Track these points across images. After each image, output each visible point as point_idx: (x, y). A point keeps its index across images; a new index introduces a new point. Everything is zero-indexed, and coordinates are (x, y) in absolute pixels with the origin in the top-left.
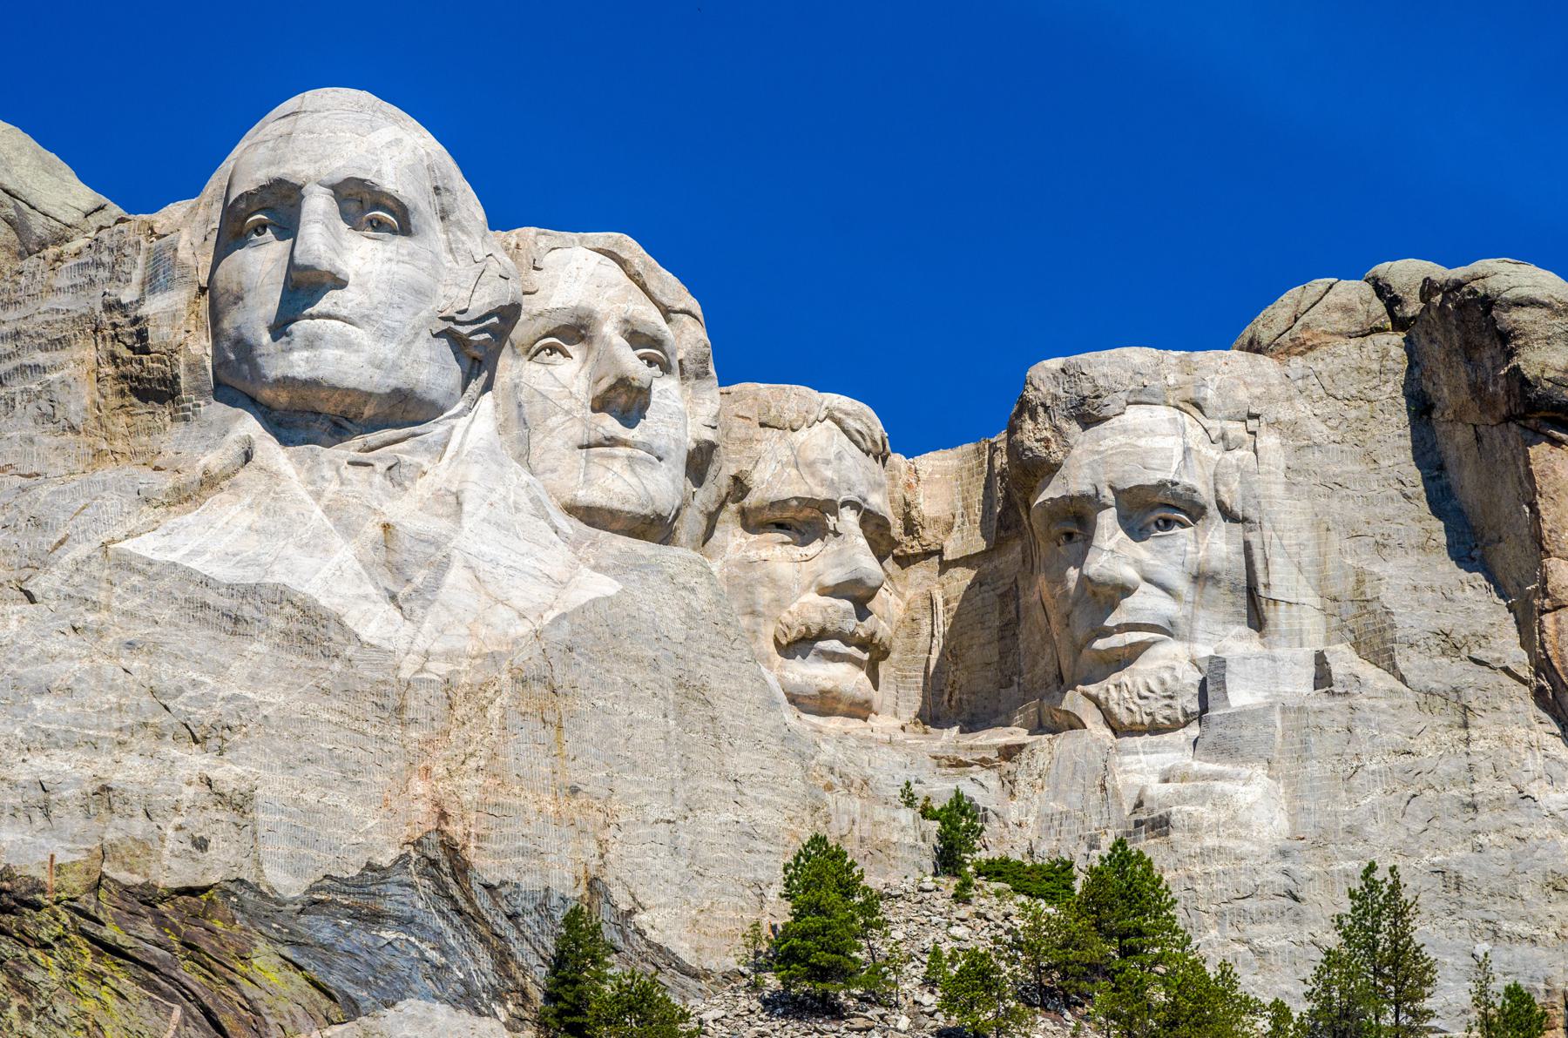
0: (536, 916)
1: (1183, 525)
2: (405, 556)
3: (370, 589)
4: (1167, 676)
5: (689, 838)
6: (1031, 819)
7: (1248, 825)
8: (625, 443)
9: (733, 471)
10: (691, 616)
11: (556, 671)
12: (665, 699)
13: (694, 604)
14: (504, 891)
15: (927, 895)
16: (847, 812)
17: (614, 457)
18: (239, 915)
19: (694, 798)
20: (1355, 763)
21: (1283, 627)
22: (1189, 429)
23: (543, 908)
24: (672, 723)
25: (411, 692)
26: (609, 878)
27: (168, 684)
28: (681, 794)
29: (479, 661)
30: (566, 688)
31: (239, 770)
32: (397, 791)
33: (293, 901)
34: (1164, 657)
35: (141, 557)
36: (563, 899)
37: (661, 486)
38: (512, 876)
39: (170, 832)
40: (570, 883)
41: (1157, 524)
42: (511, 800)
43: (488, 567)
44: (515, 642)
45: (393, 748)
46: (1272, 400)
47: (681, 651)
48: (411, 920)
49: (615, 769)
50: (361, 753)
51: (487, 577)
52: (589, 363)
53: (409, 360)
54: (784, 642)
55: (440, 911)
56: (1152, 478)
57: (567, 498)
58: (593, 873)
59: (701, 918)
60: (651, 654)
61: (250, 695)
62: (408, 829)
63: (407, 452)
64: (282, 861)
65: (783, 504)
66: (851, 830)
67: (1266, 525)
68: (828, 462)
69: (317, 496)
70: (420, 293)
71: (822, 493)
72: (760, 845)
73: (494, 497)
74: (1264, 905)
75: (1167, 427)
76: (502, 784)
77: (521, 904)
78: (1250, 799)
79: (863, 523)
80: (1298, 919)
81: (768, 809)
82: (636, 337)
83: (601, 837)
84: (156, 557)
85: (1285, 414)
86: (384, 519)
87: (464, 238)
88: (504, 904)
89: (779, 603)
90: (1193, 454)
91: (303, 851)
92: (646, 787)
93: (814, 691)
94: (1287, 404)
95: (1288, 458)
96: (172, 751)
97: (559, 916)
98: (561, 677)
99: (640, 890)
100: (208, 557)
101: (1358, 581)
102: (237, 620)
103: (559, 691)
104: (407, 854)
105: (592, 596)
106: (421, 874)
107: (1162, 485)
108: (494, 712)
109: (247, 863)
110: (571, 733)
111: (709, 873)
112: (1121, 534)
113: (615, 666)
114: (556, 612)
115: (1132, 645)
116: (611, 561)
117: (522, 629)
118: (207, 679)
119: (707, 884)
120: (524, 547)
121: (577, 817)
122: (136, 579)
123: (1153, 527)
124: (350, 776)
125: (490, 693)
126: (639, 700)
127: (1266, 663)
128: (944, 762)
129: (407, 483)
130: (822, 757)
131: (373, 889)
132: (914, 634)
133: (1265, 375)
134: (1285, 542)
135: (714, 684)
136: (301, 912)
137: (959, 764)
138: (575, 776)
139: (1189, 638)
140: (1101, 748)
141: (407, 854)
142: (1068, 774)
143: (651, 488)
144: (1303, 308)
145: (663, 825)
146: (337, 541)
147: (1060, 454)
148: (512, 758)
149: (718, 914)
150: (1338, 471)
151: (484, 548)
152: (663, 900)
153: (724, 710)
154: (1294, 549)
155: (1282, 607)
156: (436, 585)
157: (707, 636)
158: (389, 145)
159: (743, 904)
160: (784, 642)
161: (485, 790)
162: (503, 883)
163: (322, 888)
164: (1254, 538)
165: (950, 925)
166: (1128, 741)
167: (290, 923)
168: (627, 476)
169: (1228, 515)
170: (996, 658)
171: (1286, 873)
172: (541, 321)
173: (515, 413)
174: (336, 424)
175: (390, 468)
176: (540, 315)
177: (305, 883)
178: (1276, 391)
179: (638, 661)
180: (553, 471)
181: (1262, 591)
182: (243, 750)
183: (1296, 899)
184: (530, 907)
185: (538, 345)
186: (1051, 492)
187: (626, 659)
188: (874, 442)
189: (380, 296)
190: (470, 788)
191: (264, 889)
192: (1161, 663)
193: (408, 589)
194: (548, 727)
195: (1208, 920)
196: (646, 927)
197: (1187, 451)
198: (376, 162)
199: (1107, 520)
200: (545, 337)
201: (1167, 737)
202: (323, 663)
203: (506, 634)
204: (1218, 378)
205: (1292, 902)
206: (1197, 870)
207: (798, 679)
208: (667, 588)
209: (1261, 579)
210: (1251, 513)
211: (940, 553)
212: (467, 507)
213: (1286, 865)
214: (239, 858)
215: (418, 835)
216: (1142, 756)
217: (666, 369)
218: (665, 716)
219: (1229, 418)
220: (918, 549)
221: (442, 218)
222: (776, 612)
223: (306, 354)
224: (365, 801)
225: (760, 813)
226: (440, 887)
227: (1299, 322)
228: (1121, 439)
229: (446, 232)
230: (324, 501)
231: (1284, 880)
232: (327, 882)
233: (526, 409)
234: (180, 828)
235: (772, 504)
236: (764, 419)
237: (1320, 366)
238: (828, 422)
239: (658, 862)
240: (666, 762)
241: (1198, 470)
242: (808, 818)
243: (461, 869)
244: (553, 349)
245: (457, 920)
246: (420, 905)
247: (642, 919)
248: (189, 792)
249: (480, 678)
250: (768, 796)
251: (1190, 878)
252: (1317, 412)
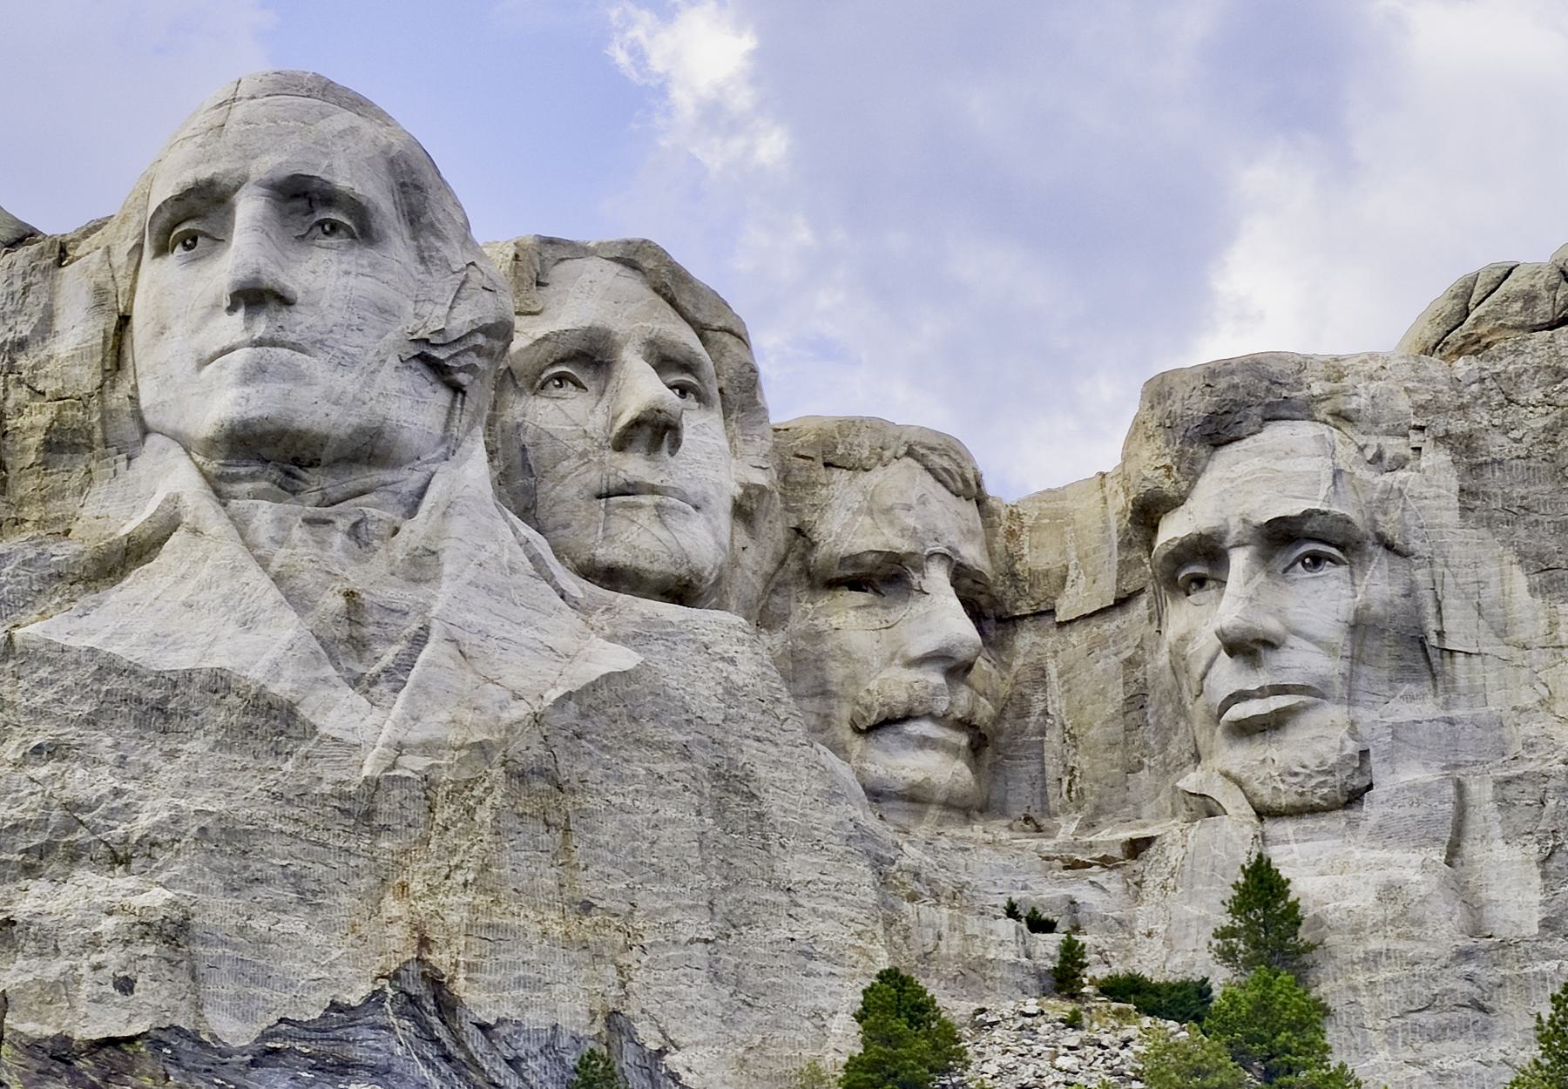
0: (542, 1060)
1: (1335, 561)
2: (372, 629)
3: (329, 671)
4: (1322, 747)
5: (733, 960)
6: (1160, 928)
7: (1420, 923)
8: (653, 490)
9: (794, 522)
10: (731, 691)
11: (561, 762)
12: (701, 794)
13: (733, 677)
14: (504, 1031)
15: (1029, 1020)
16: (931, 925)
17: (640, 506)
18: (172, 1070)
19: (739, 912)
20: (1551, 843)
21: (1462, 683)
22: (1339, 447)
23: (549, 1048)
24: (709, 821)
25: (381, 794)
26: (632, 1010)
27: (85, 793)
28: (721, 907)
29: (464, 753)
30: (575, 783)
31: (169, 895)
32: (367, 914)
33: (241, 1051)
34: (1318, 725)
35: (49, 642)
36: (576, 1039)
37: (702, 540)
38: (508, 1010)
39: (84, 970)
40: (584, 1019)
41: (1304, 564)
42: (507, 920)
43: (476, 640)
44: (510, 728)
45: (360, 862)
46: (1440, 409)
47: (718, 734)
48: (388, 1070)
49: (637, 879)
50: (320, 869)
51: (474, 652)
52: (607, 395)
53: (374, 393)
54: (863, 727)
55: (423, 1058)
56: (1294, 508)
57: (584, 557)
58: (612, 1006)
59: (750, 1056)
60: (680, 738)
61: (182, 803)
62: (382, 959)
63: (376, 506)
64: (227, 1003)
65: (854, 559)
66: (936, 947)
67: (1440, 560)
68: (909, 508)
69: (263, 562)
70: (385, 311)
71: (903, 545)
72: (821, 966)
73: (483, 556)
74: (1443, 1018)
75: (1313, 446)
76: (497, 902)
77: (522, 1047)
78: (1423, 890)
79: (956, 581)
80: (1484, 1033)
81: (830, 922)
82: (665, 361)
83: (621, 960)
84: (72, 642)
85: (1459, 426)
86: (346, 586)
87: (439, 244)
88: (502, 1046)
89: (854, 679)
90: (1345, 478)
91: (252, 991)
92: (677, 900)
93: (900, 787)
94: (1459, 414)
95: (1461, 478)
96: (84, 876)
97: (571, 1059)
98: (568, 769)
99: (673, 1024)
100: (134, 639)
101: (1551, 624)
102: (167, 716)
103: (565, 787)
104: (382, 990)
105: (605, 670)
106: (400, 1014)
107: (1308, 514)
108: (484, 815)
109: (184, 1006)
110: (581, 838)
111: (760, 1003)
112: (1261, 577)
113: (635, 753)
114: (561, 691)
115: (1277, 711)
116: (631, 629)
117: (518, 711)
118: (130, 786)
119: (757, 1015)
120: (520, 613)
121: (590, 938)
122: (44, 673)
123: (1299, 565)
124: (308, 896)
125: (478, 792)
126: (666, 795)
127: (1442, 726)
128: (1058, 863)
129: (376, 543)
130: (904, 861)
131: (339, 1033)
132: (1023, 714)
133: (1432, 379)
134: (1460, 581)
135: (761, 772)
136: (253, 1063)
137: (1074, 865)
138: (588, 886)
139: (1351, 700)
140: (1244, 838)
141: (382, 990)
142: (1205, 871)
143: (686, 542)
144: (1475, 298)
145: (700, 945)
146: (291, 616)
147: (1184, 485)
148: (507, 871)
149: (771, 1052)
150: (1523, 492)
151: (470, 617)
152: (701, 1036)
153: (774, 804)
154: (1472, 588)
155: (1460, 658)
156: (405, 664)
157: (751, 715)
158: (341, 135)
159: (800, 1038)
160: (863, 727)
161: (473, 909)
162: (500, 1021)
163: (277, 1035)
164: (1421, 576)
165: (1056, 1055)
166: (1275, 828)
167: (237, 1078)
168: (656, 529)
169: (1389, 547)
170: (1122, 737)
171: (1469, 978)
172: (548, 346)
173: (518, 460)
174: (288, 473)
175: (355, 525)
176: (546, 338)
177: (255, 1030)
178: (1445, 398)
179: (662, 747)
180: (566, 526)
181: (1433, 640)
182: (178, 869)
183: (1482, 1009)
184: (535, 1049)
185: (544, 376)
186: (1173, 529)
187: (649, 745)
188: (965, 481)
189: (335, 317)
190: (456, 908)
191: (205, 1037)
192: (1314, 732)
193: (375, 669)
194: (553, 831)
195: (1375, 1038)
196: (681, 1070)
197: (1337, 474)
198: (326, 155)
199: (1239, 560)
200: (552, 365)
201: (1324, 822)
202: (269, 763)
203: (498, 719)
204: (1374, 386)
205: (1479, 1015)
206: (1361, 979)
207: (881, 772)
208: (700, 659)
209: (1432, 625)
210: (1415, 545)
211: (1052, 612)
212: (448, 569)
213: (1470, 968)
214: (173, 1002)
215: (394, 966)
216: (1294, 846)
217: (702, 398)
218: (699, 813)
219: (1387, 433)
220: (1025, 608)
221: (412, 222)
222: (851, 690)
223: (247, 390)
224: (329, 927)
225: (819, 926)
226: (423, 1029)
227: (1473, 316)
228: (1256, 462)
229: (414, 238)
230: (274, 567)
231: (1466, 987)
232: (283, 1027)
233: (531, 454)
234: (97, 968)
235: (843, 559)
236: (830, 458)
237: (1499, 367)
238: (909, 460)
239: (697, 990)
240: (702, 869)
241: (1352, 497)
242: (880, 932)
243: (447, 1006)
244: (562, 378)
245: (445, 1068)
246: (399, 1050)
247: (674, 1060)
248: (108, 924)
249: (466, 774)
250: (830, 906)
251: (1355, 989)
252: (1496, 422)
